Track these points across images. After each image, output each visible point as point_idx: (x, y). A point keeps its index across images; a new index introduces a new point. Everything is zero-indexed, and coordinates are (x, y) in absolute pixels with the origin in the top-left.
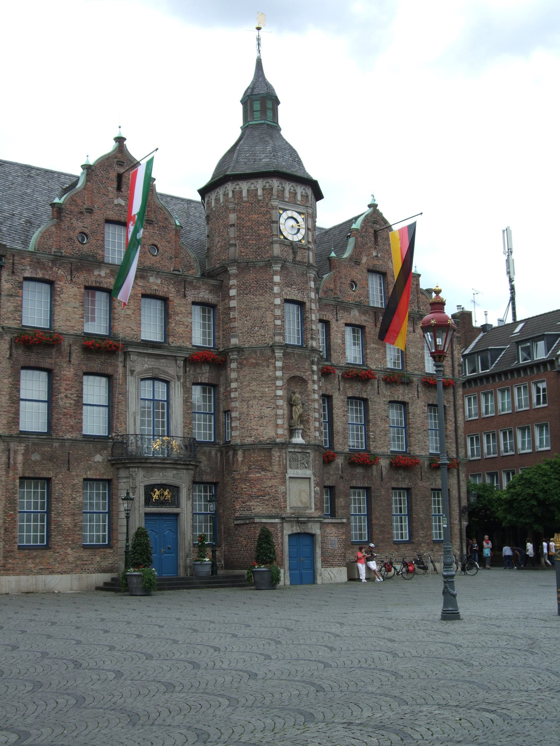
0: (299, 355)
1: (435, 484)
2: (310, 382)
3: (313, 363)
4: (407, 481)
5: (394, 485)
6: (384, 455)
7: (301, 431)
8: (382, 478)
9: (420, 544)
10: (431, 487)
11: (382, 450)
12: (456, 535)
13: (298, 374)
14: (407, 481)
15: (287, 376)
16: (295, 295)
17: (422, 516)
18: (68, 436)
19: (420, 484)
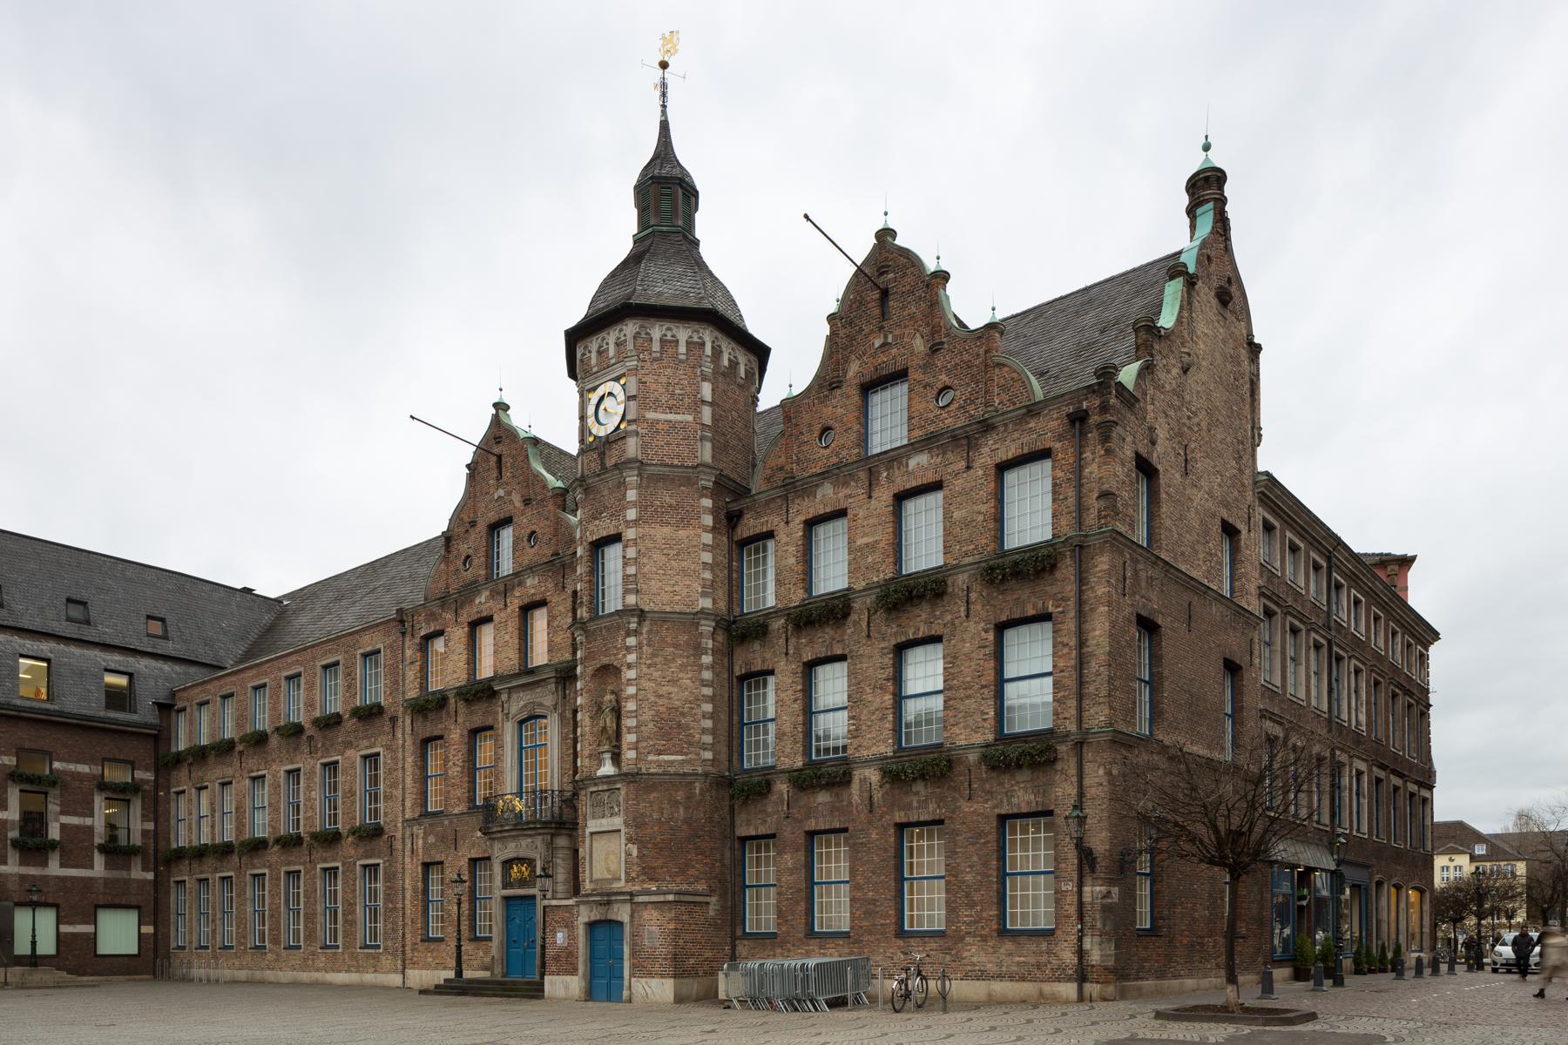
0: (608, 629)
1: (1010, 803)
2: (624, 669)
3: (628, 634)
4: (932, 807)
5: (900, 817)
6: (867, 763)
7: (607, 756)
8: (871, 804)
9: (962, 939)
10: (997, 811)
11: (874, 750)
12: (1068, 917)
13: (605, 661)
14: (932, 807)
15: (590, 670)
16: (604, 528)
17: (968, 877)
18: (456, 811)
19: (966, 807)
